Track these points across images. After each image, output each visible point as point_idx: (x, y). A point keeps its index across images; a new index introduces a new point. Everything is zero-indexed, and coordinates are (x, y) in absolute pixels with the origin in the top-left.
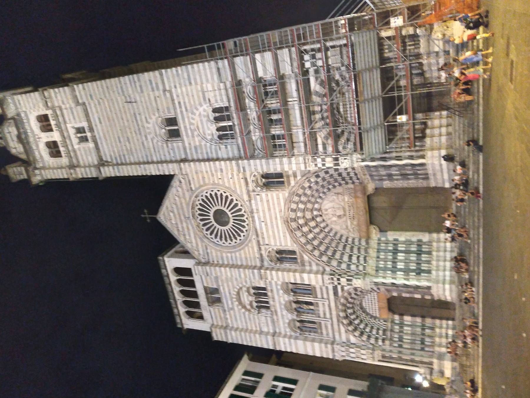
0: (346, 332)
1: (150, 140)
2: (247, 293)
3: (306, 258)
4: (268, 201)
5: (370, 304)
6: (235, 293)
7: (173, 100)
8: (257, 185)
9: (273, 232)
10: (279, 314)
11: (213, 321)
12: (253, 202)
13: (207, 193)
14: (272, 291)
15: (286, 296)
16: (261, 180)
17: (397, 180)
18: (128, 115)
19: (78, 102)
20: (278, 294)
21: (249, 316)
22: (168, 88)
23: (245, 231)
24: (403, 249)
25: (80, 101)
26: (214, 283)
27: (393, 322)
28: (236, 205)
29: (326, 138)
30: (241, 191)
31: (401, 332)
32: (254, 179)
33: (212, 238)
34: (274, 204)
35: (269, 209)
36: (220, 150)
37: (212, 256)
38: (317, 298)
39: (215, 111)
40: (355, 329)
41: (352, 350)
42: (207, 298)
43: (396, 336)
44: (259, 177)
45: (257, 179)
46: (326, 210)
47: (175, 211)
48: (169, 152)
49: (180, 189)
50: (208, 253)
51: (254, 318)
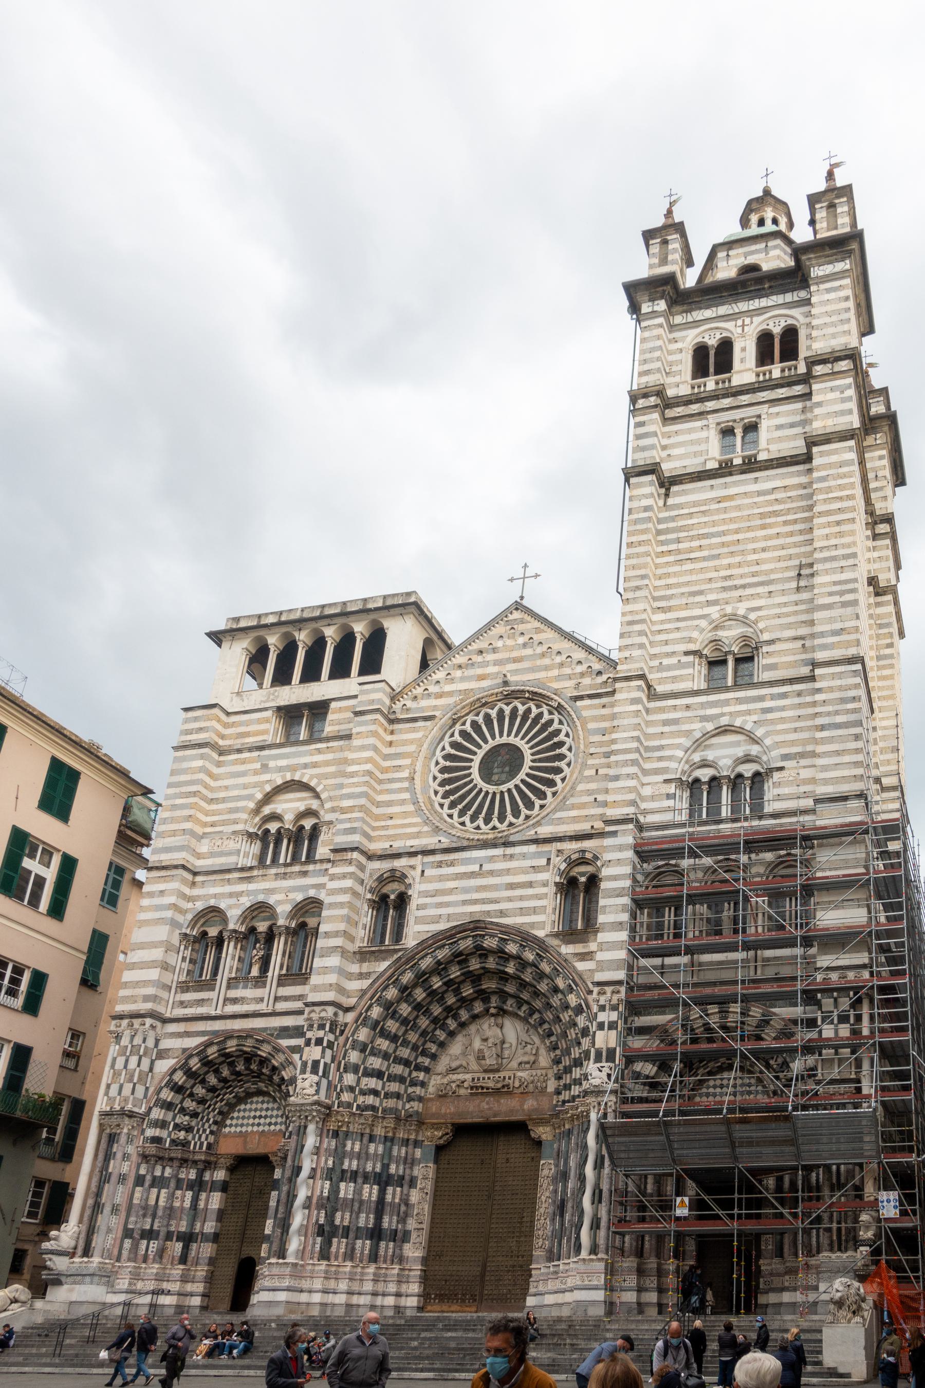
1: (707, 610)
3: (384, 965)
4: (530, 884)
8: (572, 864)
9: (451, 891)
12: (533, 848)
13: (567, 735)
16: (582, 874)
18: (771, 566)
23: (461, 820)
28: (530, 805)
30: (561, 821)
31: (179, 1184)
33: (452, 735)
34: (521, 898)
35: (511, 886)
36: (667, 781)
43: (168, 1172)
44: (589, 869)
45: (588, 864)
49: (579, 669)
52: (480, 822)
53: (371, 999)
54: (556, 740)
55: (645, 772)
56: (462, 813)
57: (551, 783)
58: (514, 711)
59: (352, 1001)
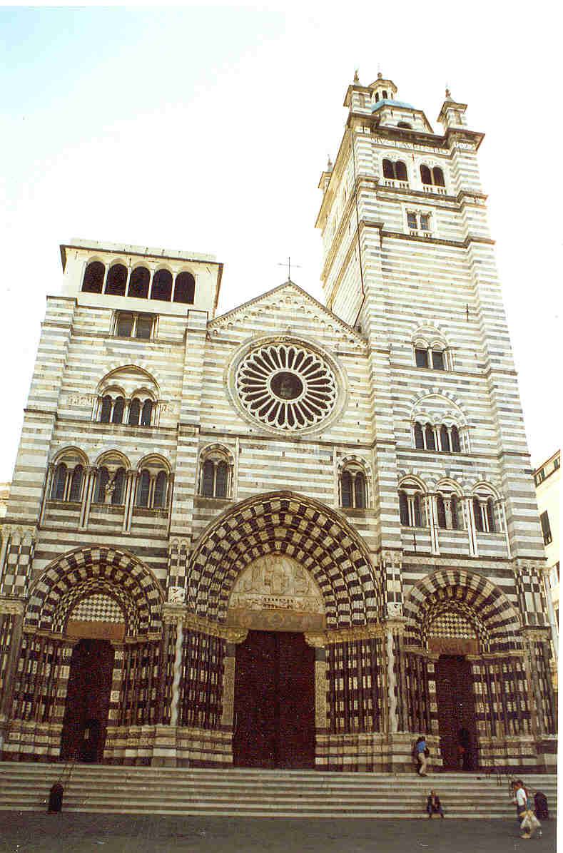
0: (58, 554)
2: (139, 387)
4: (321, 472)
5: (99, 608)
6: (143, 367)
7: (473, 375)
10: (98, 436)
11: (83, 307)
14: (149, 436)
15: (138, 458)
16: (354, 471)
17: (332, 684)
18: (450, 302)
19: (472, 240)
20: (141, 445)
21: (95, 379)
22: (493, 375)
24: (213, 680)
25: (472, 243)
26: (165, 335)
27: (61, 644)
28: (311, 418)
29: (422, 588)
30: (337, 433)
32: (358, 459)
33: (249, 358)
35: (307, 471)
36: (404, 420)
37: (219, 349)
38: (133, 515)
39: (455, 430)
40: (60, 571)
41: (24, 559)
42: (131, 313)
45: (357, 464)
46: (281, 563)
47: (300, 315)
48: (398, 341)
49: (338, 335)
50: (226, 342)
51: (87, 386)
52: (276, 421)
53: (209, 535)
54: (323, 377)
55: (395, 413)
56: (262, 413)
57: (324, 406)
58: (292, 352)
59: (196, 535)
